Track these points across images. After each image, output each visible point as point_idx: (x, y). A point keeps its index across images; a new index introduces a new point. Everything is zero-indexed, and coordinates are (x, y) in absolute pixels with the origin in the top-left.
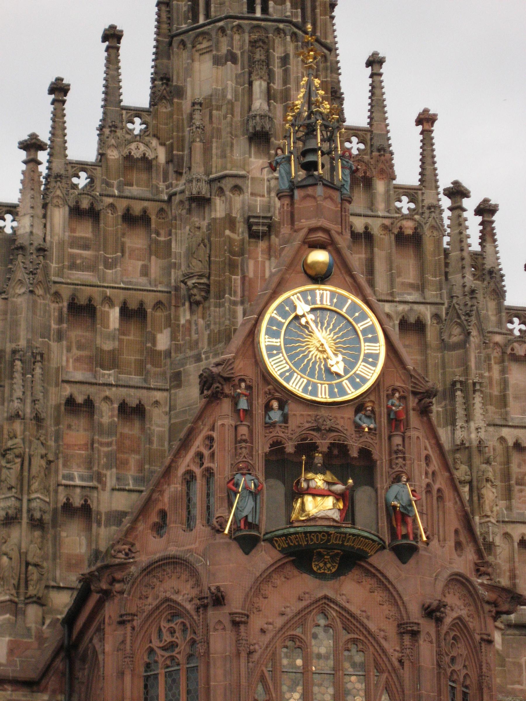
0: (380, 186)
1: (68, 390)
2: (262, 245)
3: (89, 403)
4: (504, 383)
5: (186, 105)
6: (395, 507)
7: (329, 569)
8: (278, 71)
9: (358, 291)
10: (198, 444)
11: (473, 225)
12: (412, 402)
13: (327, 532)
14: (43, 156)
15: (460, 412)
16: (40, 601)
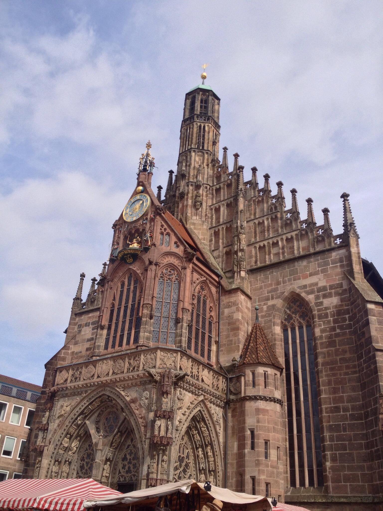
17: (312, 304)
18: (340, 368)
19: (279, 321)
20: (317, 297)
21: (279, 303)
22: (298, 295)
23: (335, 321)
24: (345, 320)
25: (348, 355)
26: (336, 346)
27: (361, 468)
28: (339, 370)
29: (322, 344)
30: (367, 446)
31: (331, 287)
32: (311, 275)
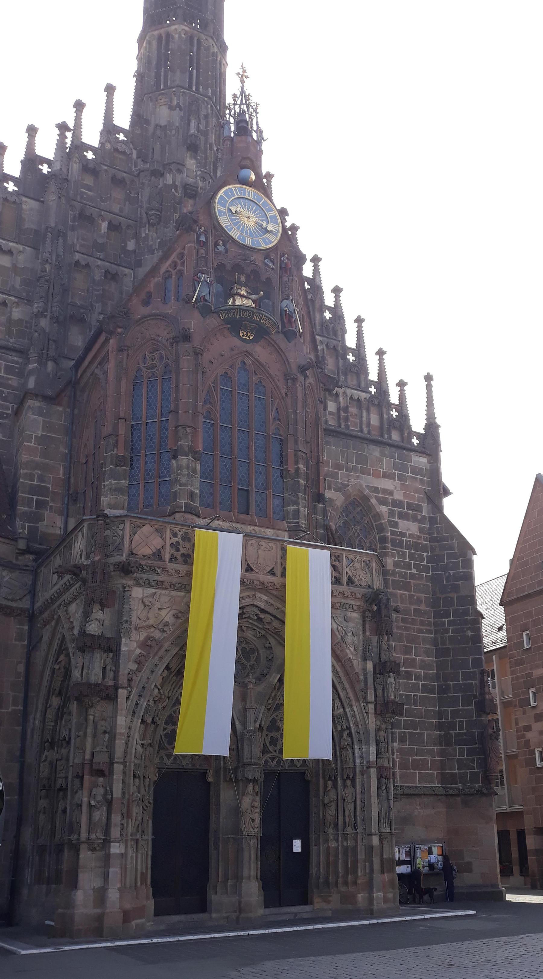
6: (286, 311)
7: (249, 337)
13: (252, 311)
18: (414, 622)
25: (423, 607)
26: (411, 592)
27: (431, 752)
28: (413, 624)
30: (440, 726)
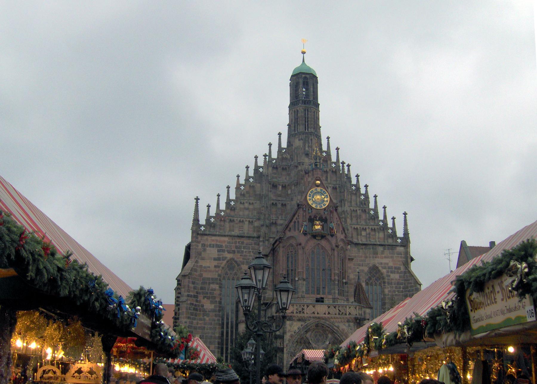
0: (329, 162)
1: (272, 201)
2: (307, 175)
3: (276, 204)
4: (351, 199)
5: (294, 147)
8: (310, 142)
9: (325, 188)
10: (296, 216)
11: (346, 168)
12: (334, 208)
14: (267, 157)
15: (343, 205)
16: (268, 240)
17: (385, 275)
19: (364, 280)
20: (388, 272)
21: (366, 269)
22: (377, 268)
23: (396, 288)
24: (400, 288)
29: (388, 298)
31: (395, 268)
32: (385, 257)
